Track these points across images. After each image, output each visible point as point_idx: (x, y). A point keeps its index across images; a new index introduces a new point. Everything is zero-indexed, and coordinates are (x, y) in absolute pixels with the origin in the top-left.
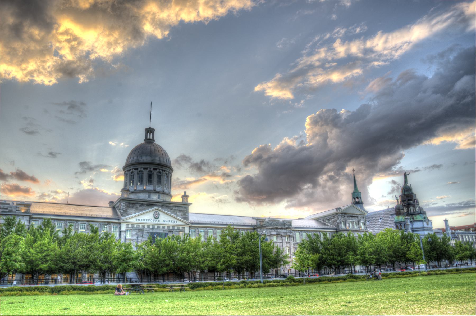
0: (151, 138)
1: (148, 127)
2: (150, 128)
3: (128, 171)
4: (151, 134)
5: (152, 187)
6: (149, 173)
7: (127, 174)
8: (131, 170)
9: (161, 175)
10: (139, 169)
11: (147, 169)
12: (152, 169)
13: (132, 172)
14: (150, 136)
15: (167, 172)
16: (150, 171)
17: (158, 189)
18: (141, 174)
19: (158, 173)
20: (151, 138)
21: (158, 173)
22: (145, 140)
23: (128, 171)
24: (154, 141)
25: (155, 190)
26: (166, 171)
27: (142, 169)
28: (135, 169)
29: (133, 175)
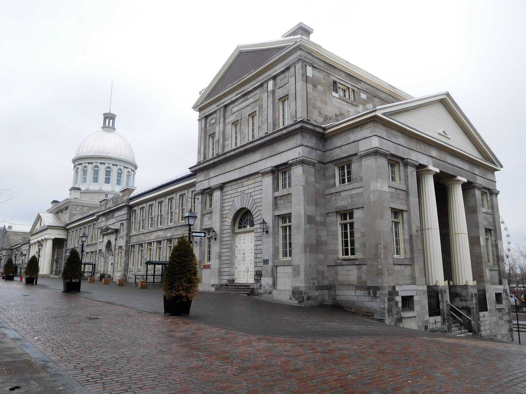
0: (111, 125)
1: (108, 112)
3: (79, 164)
4: (111, 121)
7: (78, 168)
8: (84, 165)
10: (94, 164)
13: (85, 167)
15: (130, 170)
22: (102, 128)
23: (79, 164)
24: (115, 130)
26: (129, 168)
27: (99, 164)
28: (89, 163)
29: (87, 170)
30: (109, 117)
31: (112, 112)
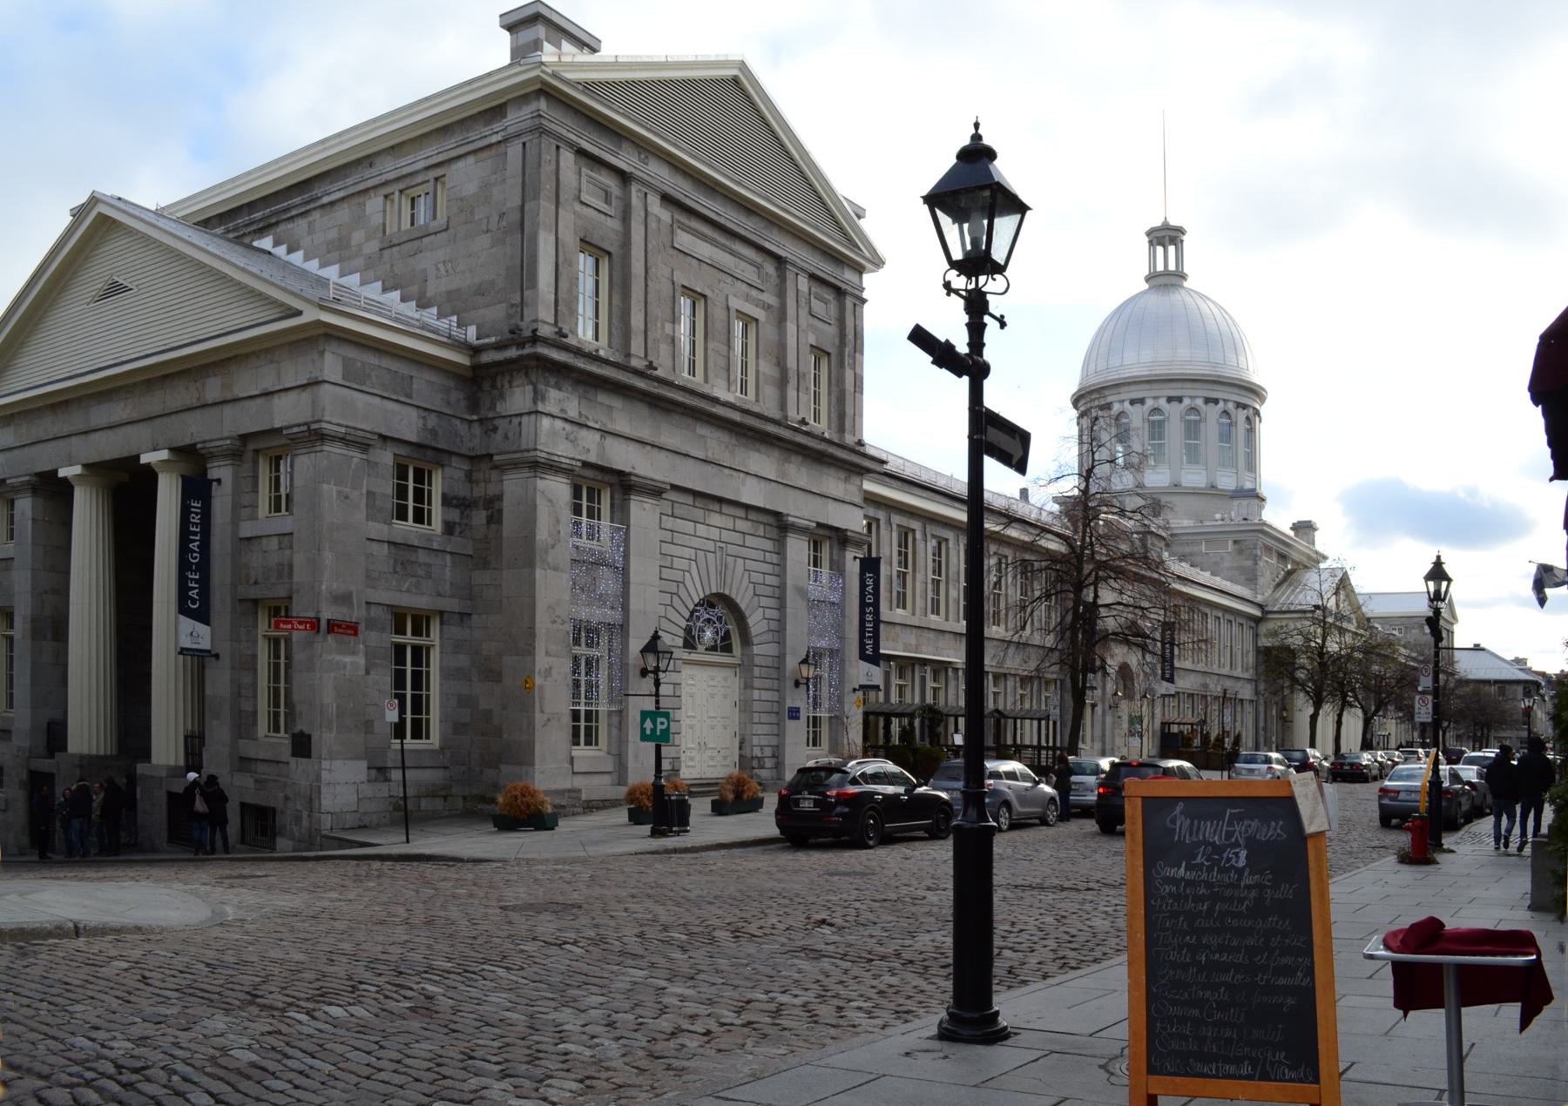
1: (1158, 223)
2: (1166, 227)
5: (1168, 471)
6: (1151, 418)
9: (1200, 421)
11: (1142, 401)
12: (1200, 402)
14: (1165, 259)
16: (1156, 410)
17: (1224, 479)
18: (1195, 421)
19: (1186, 414)
20: (1172, 267)
21: (1186, 414)
24: (1183, 277)
25: (1213, 487)
30: (1166, 236)
31: (1173, 222)
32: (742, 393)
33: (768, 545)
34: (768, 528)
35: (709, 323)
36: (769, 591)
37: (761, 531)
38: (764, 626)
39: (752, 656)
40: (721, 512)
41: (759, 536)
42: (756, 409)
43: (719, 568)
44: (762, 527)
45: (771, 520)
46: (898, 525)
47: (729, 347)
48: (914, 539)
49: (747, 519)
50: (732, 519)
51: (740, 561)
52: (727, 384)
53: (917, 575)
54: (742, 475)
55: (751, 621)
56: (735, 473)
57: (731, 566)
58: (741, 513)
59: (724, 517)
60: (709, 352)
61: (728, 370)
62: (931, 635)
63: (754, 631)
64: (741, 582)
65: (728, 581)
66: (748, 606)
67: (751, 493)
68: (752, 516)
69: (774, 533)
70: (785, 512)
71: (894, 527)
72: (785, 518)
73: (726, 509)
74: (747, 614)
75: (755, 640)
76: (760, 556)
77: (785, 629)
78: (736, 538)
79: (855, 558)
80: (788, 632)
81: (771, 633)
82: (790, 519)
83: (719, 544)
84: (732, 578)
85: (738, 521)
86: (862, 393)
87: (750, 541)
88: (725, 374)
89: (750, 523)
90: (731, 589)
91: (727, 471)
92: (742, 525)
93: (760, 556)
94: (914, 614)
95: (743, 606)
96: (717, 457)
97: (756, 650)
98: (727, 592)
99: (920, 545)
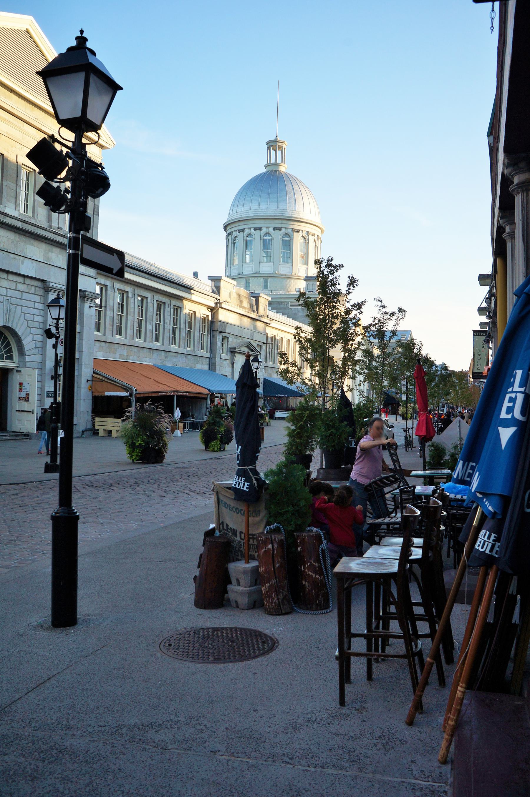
32: (24, 212)
33: (37, 298)
34: (37, 289)
35: (4, 170)
36: (37, 325)
37: (33, 290)
38: (33, 345)
39: (25, 362)
40: (7, 279)
41: (32, 293)
42: (33, 221)
43: (5, 311)
44: (33, 288)
45: (39, 284)
46: (118, 289)
47: (17, 184)
48: (128, 297)
49: (24, 283)
50: (14, 283)
51: (19, 308)
52: (14, 206)
53: (129, 317)
54: (22, 258)
55: (24, 342)
56: (17, 257)
57: (13, 310)
58: (21, 279)
59: (10, 282)
60: (4, 187)
61: (16, 198)
62: (136, 349)
63: (26, 348)
64: (19, 320)
65: (11, 319)
66: (23, 334)
67: (28, 269)
68: (28, 281)
69: (41, 292)
70: (48, 280)
71: (116, 290)
72: (47, 284)
73: (11, 277)
74: (22, 338)
75: (27, 353)
76: (31, 304)
77: (46, 347)
78: (18, 294)
79: (90, 307)
80: (47, 348)
81: (37, 349)
82: (51, 284)
83: (5, 297)
84: (14, 318)
85: (18, 285)
86: (98, 215)
87: (25, 296)
88: (14, 200)
89: (26, 286)
90: (12, 324)
91: (12, 256)
92: (20, 287)
93: (31, 304)
94: (126, 338)
95: (20, 334)
96: (5, 247)
97: (27, 358)
98: (10, 325)
99: (131, 301)
